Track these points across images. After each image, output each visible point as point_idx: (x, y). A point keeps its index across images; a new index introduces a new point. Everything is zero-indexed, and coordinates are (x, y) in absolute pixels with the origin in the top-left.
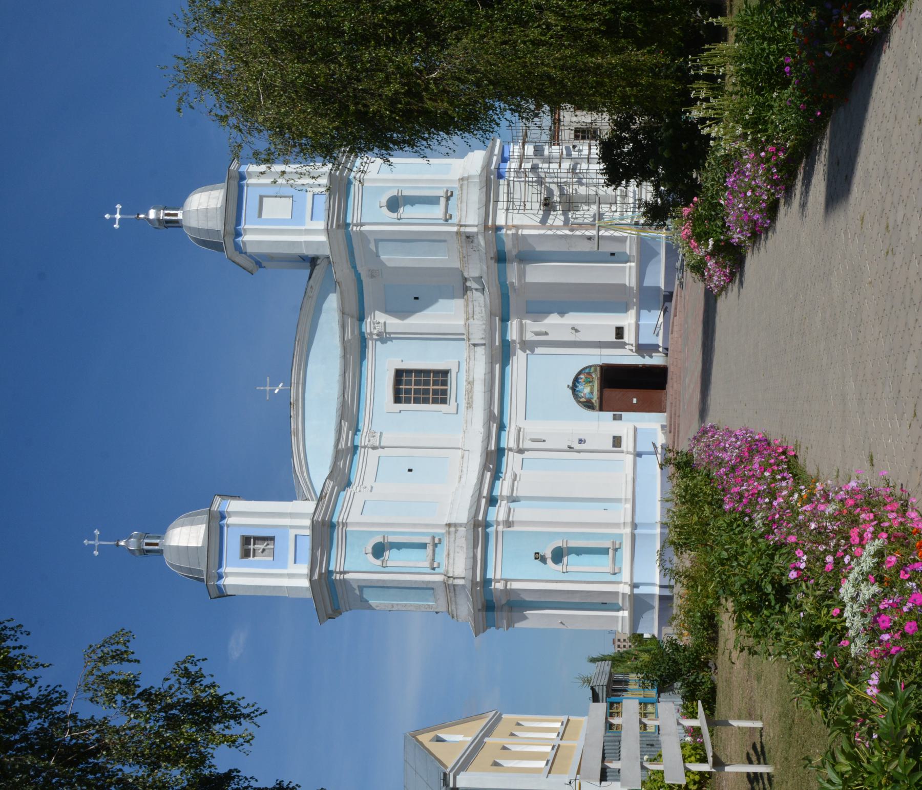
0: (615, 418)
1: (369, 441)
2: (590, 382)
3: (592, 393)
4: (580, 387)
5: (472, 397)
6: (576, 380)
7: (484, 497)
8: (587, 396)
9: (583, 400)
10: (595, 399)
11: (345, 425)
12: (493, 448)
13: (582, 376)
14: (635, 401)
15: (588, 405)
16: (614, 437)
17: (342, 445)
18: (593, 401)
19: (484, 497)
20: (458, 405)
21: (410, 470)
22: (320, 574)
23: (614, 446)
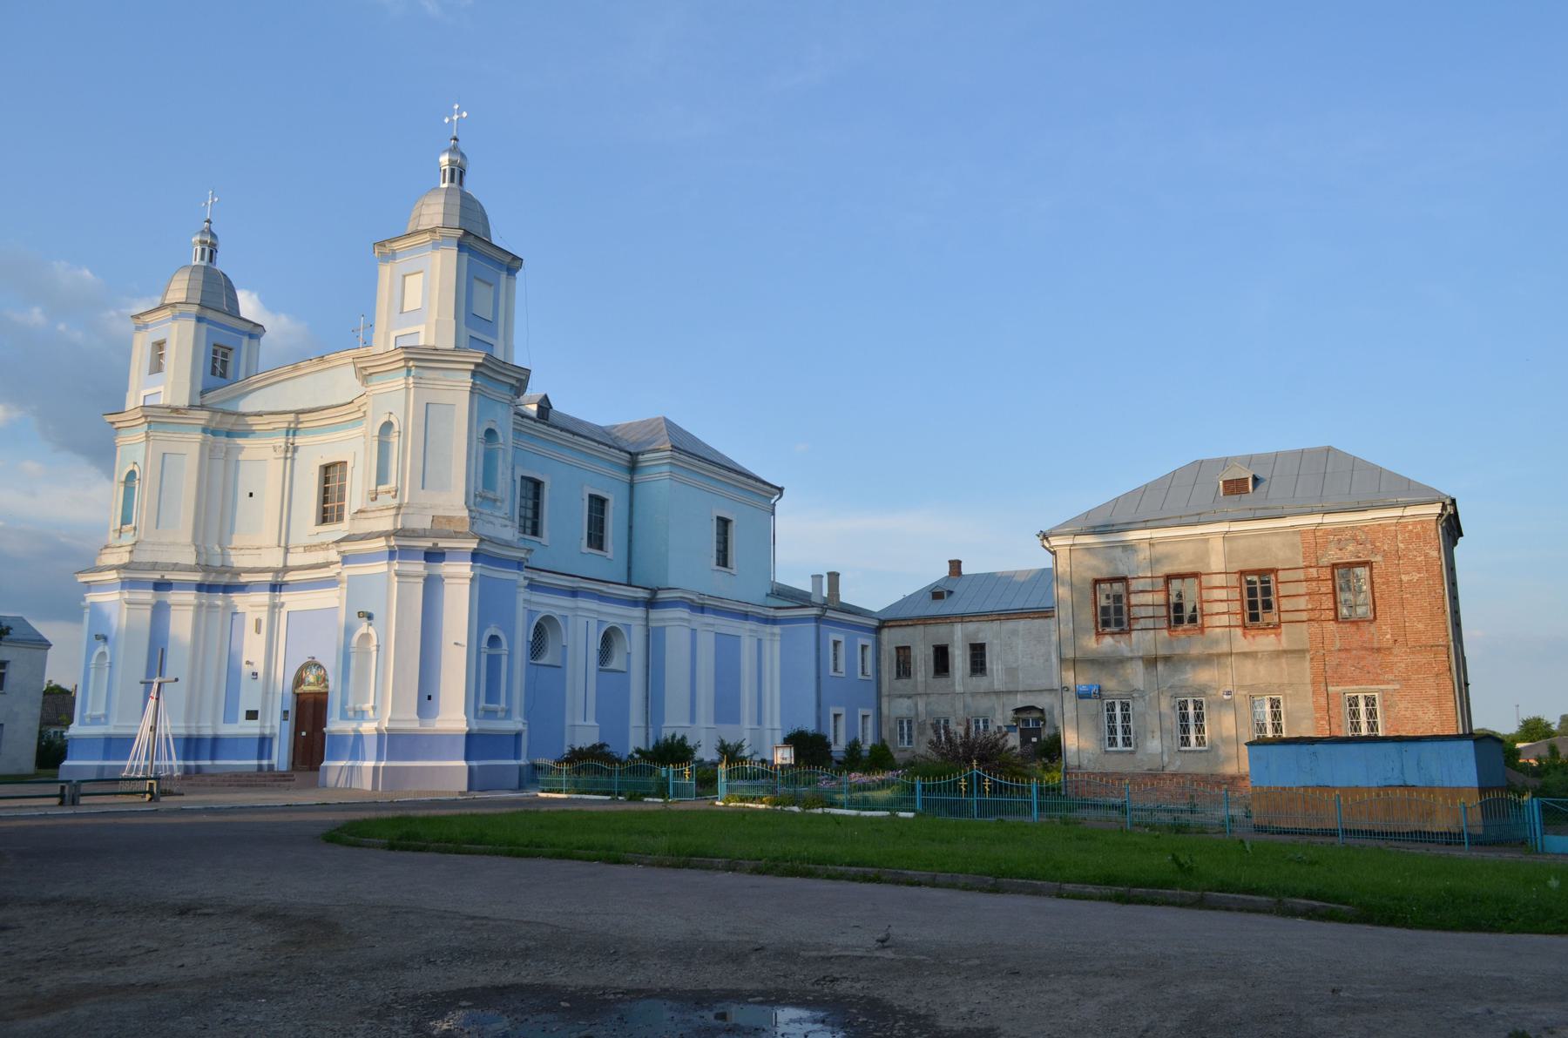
0: (286, 713)
2: (318, 681)
3: (308, 685)
4: (314, 670)
6: (320, 667)
7: (163, 576)
8: (307, 680)
9: (304, 675)
10: (305, 688)
13: (323, 672)
14: (304, 734)
15: (299, 680)
16: (256, 712)
18: (302, 686)
21: (251, 495)
22: (113, 423)
23: (248, 712)
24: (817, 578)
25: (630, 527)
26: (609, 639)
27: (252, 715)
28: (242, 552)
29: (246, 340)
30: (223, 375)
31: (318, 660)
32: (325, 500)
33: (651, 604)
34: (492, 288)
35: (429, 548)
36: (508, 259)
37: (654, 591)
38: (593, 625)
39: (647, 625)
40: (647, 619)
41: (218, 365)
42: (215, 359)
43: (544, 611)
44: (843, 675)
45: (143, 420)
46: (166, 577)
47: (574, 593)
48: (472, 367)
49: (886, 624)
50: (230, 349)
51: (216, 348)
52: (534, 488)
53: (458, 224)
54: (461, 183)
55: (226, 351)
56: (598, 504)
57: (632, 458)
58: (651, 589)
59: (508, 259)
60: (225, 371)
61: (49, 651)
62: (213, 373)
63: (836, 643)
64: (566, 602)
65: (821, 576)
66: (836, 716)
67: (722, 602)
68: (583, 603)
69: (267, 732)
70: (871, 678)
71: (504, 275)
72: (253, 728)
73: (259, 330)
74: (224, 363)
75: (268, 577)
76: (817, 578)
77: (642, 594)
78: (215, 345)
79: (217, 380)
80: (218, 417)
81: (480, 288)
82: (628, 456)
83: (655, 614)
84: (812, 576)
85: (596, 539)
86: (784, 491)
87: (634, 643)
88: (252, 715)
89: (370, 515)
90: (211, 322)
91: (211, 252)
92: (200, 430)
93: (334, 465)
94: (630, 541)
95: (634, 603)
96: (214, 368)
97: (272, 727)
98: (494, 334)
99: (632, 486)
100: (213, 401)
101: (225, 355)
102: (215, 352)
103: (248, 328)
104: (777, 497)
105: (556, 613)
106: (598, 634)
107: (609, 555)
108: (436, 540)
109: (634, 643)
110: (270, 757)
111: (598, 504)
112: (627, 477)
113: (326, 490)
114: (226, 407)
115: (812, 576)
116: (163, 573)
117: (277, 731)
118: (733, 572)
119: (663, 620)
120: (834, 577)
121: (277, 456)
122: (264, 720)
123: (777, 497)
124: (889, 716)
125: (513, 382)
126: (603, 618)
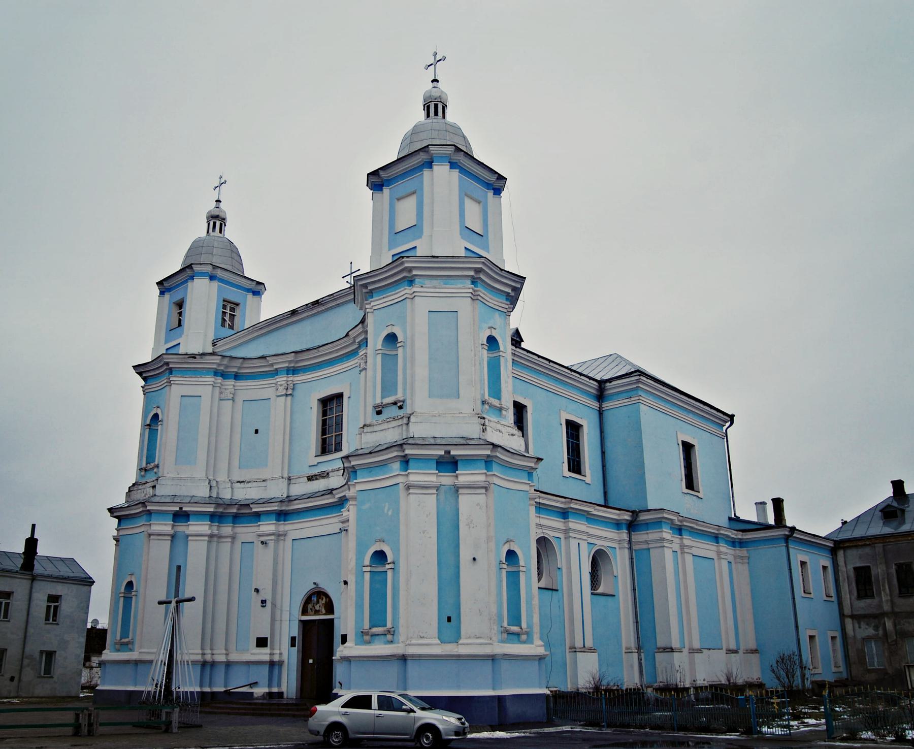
0: (293, 639)
1: (281, 385)
5: (317, 479)
7: (181, 508)
11: (291, 357)
12: (254, 510)
17: (271, 360)
19: (181, 508)
20: (317, 465)
21: (257, 432)
24: (761, 505)
25: (603, 453)
26: (598, 561)
27: (262, 642)
28: (250, 485)
29: (250, 296)
30: (231, 327)
32: (324, 432)
33: (632, 526)
37: (635, 513)
38: (584, 545)
39: (630, 548)
40: (630, 541)
41: (227, 318)
42: (224, 313)
44: (812, 596)
46: (184, 509)
48: (472, 273)
49: (842, 545)
50: (237, 305)
51: (226, 303)
52: (520, 409)
54: (444, 117)
55: (233, 306)
56: (573, 429)
57: (600, 386)
58: (631, 512)
61: (92, 587)
62: (223, 325)
63: (803, 564)
65: (764, 503)
66: (812, 638)
67: (697, 525)
68: (575, 524)
69: (276, 658)
70: (833, 599)
71: (490, 194)
72: (263, 654)
73: (260, 287)
74: (232, 317)
75: (275, 507)
76: (761, 505)
77: (627, 517)
78: (224, 301)
79: (227, 332)
80: (226, 361)
83: (639, 537)
84: (756, 504)
85: (575, 465)
86: (735, 418)
87: (620, 562)
88: (262, 642)
89: (376, 428)
90: (222, 280)
91: (221, 225)
92: (213, 374)
94: (604, 466)
95: (617, 525)
96: (224, 320)
97: (281, 654)
99: (601, 413)
101: (233, 310)
102: (224, 307)
103: (252, 286)
104: (728, 424)
105: (550, 534)
106: (589, 557)
107: (588, 479)
108: (448, 448)
109: (620, 562)
110: (279, 685)
111: (573, 429)
113: (324, 422)
114: (234, 354)
115: (756, 504)
116: (181, 505)
117: (285, 657)
118: (700, 495)
119: (647, 542)
120: (778, 504)
121: (279, 394)
122: (272, 648)
123: (728, 424)
124: (855, 636)
125: (509, 290)
126: (590, 541)
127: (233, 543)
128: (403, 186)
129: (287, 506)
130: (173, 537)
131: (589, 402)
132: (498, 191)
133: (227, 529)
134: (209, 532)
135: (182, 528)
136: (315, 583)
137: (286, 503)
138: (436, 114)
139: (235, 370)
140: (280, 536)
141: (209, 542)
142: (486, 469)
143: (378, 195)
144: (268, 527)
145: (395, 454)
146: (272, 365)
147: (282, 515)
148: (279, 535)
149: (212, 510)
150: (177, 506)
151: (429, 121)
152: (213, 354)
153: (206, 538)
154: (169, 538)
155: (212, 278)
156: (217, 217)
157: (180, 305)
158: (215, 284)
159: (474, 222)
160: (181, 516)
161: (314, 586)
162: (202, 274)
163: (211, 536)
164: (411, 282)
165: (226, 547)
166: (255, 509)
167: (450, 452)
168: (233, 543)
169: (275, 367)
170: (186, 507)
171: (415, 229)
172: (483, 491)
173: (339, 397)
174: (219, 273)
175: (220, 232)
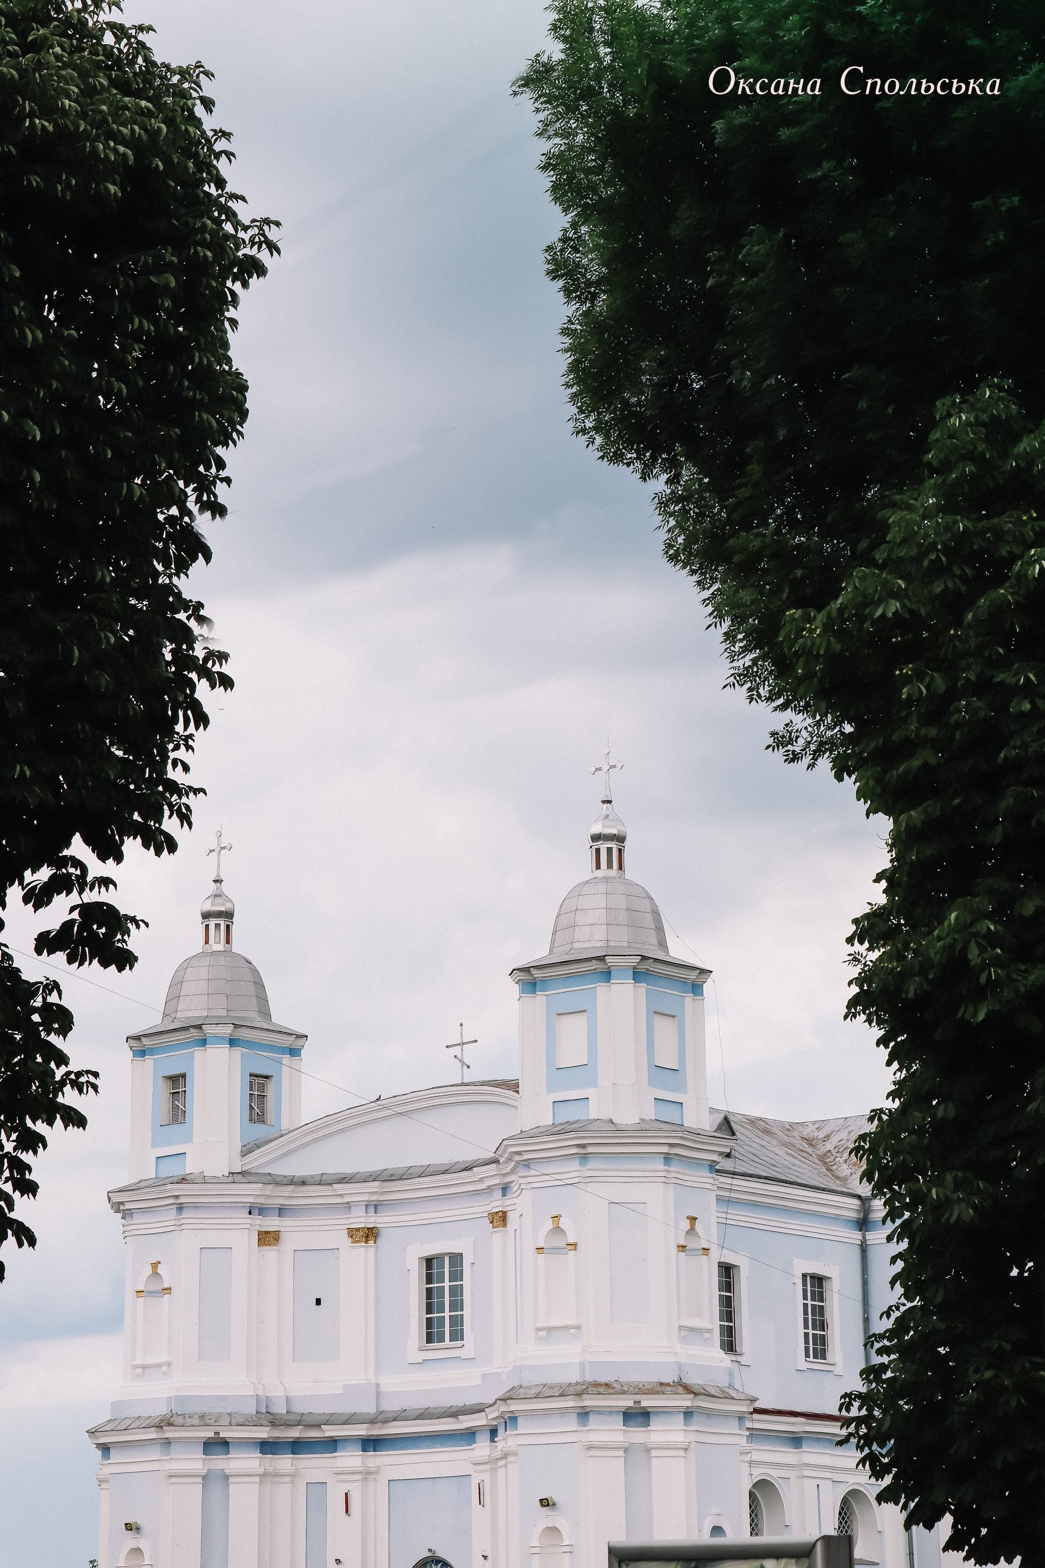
12: (327, 1434)
21: (318, 1302)
29: (286, 1059)
31: (441, 1554)
34: (676, 1020)
35: (630, 1408)
36: (693, 975)
38: (826, 1486)
43: (758, 1474)
45: (171, 1201)
47: (796, 1440)
50: (267, 1077)
53: (626, 939)
54: (620, 868)
55: (261, 1080)
56: (816, 1284)
59: (693, 975)
60: (263, 1113)
64: (786, 1455)
71: (689, 999)
73: (302, 1041)
78: (251, 1075)
79: (259, 1131)
81: (663, 1026)
82: (856, 1202)
93: (440, 1257)
98: (682, 1088)
100: (260, 1162)
105: (773, 1474)
107: (838, 1370)
108: (638, 1397)
111: (816, 1284)
112: (856, 1236)
116: (217, 1429)
127: (293, 1482)
128: (567, 995)
129: (380, 1428)
130: (204, 1478)
131: (843, 1235)
132: (696, 989)
133: (284, 1462)
134: (261, 1470)
135: (219, 1462)
136: (430, 1550)
137: (379, 1425)
138: (610, 866)
139: (282, 1201)
140: (368, 1474)
141: (261, 1482)
142: (685, 1425)
143: (528, 999)
144: (350, 1459)
145: (571, 1404)
146: (341, 1195)
147: (371, 1444)
148: (369, 1473)
149: (265, 1435)
150: (211, 1431)
151: (599, 873)
152: (245, 1175)
153: (257, 1479)
154: (200, 1480)
155: (232, 1042)
156: (219, 914)
157: (177, 1081)
158: (238, 1052)
159: (667, 1058)
160: (217, 1445)
161: (430, 1554)
162: (218, 1039)
163: (263, 1476)
164: (584, 1158)
165: (284, 1490)
166: (330, 1431)
167: (639, 1402)
168: (293, 1482)
169: (347, 1199)
170: (223, 1431)
171: (585, 1072)
172: (682, 1453)
173: (456, 1259)
174: (243, 1033)
175: (228, 941)
